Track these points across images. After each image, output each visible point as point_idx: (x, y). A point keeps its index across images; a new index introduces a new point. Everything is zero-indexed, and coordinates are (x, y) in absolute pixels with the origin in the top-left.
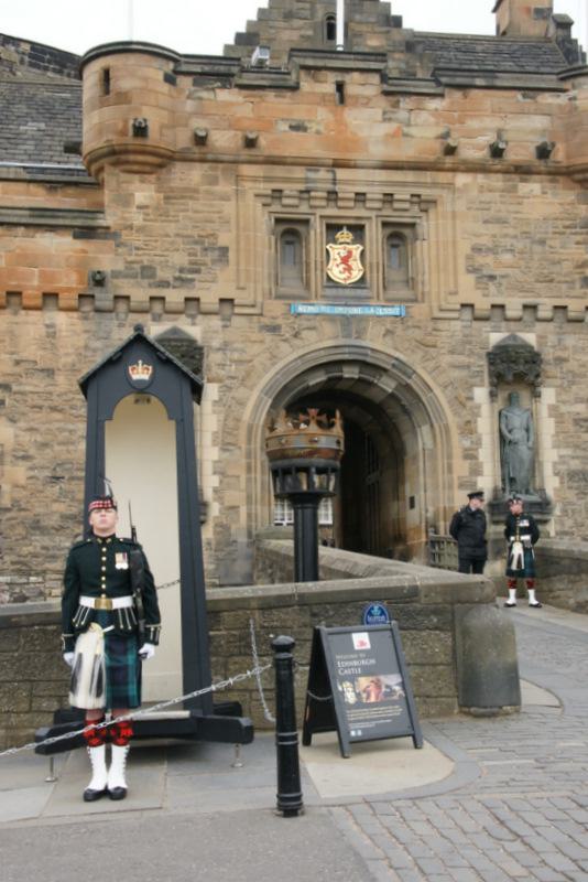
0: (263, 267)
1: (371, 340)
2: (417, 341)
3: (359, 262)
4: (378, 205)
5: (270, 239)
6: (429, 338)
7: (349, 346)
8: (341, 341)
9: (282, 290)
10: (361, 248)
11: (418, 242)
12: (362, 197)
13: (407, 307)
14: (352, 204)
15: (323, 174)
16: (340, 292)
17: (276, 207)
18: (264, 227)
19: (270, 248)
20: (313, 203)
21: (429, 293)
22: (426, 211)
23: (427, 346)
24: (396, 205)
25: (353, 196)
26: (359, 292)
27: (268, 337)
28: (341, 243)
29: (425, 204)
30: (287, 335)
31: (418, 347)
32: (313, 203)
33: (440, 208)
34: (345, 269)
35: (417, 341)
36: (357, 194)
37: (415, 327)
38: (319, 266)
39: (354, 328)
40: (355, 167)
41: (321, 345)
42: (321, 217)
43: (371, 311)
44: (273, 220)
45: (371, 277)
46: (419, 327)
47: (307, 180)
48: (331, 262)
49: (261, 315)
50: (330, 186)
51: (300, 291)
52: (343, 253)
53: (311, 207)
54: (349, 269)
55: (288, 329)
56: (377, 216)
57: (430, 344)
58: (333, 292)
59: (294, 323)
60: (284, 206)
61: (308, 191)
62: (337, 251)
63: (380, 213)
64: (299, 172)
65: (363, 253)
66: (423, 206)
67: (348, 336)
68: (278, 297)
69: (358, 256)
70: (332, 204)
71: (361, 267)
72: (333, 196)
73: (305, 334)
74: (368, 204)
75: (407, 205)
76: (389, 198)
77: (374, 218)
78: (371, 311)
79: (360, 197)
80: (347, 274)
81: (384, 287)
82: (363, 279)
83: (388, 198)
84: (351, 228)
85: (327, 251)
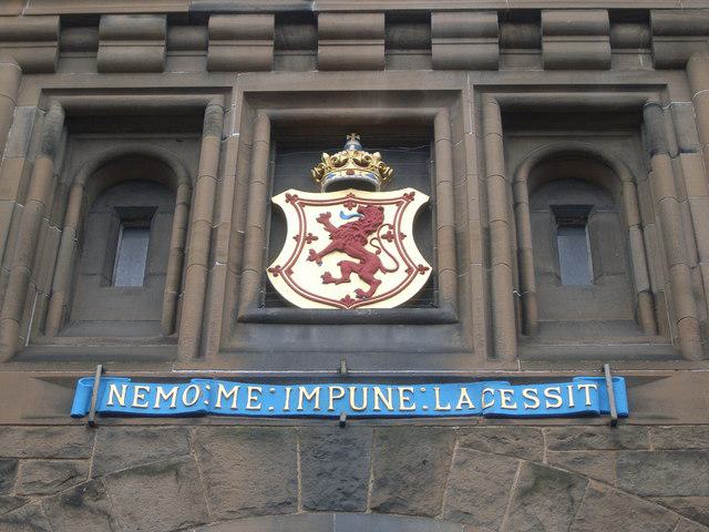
1: (461, 516)
3: (410, 243)
4: (489, 50)
5: (30, 170)
9: (63, 343)
10: (421, 199)
11: (661, 162)
13: (631, 383)
14: (376, 51)
20: (219, 52)
24: (553, 48)
26: (404, 336)
32: (219, 52)
34: (347, 269)
37: (675, 453)
38: (223, 245)
39: (371, 464)
42: (252, 98)
44: (56, 112)
45: (459, 284)
52: (340, 216)
53: (215, 68)
54: (368, 268)
55: (43, 475)
56: (479, 89)
58: (289, 336)
59: (74, 448)
60: (105, 69)
62: (312, 213)
65: (424, 218)
66: (664, 48)
69: (407, 226)
70: (299, 59)
71: (418, 258)
72: (302, 33)
73: (120, 494)
74: (441, 50)
75: (601, 48)
76: (526, 31)
77: (468, 95)
81: (524, 328)
84: (374, 136)
85: (277, 216)
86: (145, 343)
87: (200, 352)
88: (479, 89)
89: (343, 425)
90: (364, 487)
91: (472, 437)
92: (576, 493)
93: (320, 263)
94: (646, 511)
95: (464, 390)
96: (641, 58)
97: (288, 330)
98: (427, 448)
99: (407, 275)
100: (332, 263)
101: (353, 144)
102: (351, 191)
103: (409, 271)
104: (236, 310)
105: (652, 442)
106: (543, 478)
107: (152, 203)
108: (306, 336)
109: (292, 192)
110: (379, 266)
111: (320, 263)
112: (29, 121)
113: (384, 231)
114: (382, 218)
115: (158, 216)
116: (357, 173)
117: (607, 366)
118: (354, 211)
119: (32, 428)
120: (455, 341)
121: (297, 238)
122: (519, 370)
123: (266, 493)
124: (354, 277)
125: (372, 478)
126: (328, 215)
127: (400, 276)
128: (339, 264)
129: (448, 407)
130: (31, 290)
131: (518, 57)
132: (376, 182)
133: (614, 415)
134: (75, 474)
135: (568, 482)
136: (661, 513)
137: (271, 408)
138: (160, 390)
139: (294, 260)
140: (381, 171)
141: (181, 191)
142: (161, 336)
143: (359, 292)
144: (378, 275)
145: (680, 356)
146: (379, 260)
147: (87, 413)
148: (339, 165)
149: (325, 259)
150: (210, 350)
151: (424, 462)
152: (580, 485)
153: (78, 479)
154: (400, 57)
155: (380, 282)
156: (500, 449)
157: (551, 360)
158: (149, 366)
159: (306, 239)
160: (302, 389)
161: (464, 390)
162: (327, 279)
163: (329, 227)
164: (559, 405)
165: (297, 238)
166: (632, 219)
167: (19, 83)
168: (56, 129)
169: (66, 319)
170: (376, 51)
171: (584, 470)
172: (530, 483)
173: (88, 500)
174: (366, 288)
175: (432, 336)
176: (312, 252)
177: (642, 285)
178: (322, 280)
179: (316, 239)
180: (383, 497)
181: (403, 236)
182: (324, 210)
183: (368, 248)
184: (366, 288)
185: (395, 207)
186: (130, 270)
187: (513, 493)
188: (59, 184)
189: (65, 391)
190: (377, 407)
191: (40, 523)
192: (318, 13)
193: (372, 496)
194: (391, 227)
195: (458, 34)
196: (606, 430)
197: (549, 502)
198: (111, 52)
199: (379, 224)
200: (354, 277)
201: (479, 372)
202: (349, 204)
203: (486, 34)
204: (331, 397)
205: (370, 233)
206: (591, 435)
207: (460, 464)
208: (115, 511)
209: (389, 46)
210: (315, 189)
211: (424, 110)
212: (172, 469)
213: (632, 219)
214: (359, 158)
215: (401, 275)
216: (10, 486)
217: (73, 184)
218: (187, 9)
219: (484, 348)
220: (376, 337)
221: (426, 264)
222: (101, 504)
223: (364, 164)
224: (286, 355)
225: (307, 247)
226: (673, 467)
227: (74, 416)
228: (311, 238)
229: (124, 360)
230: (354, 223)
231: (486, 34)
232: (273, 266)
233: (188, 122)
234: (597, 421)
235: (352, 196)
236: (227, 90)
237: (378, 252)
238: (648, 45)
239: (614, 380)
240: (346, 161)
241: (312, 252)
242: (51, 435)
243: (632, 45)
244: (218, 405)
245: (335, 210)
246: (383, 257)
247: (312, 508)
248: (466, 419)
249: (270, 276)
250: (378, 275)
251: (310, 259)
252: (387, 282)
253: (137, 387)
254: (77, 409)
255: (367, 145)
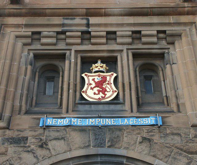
0: (16, 88)
1: (127, 148)
2: (176, 147)
3: (113, 85)
4: (129, 40)
5: (26, 69)
6: (190, 145)
7: (101, 155)
8: (92, 151)
9: (36, 109)
10: (115, 75)
11: (168, 66)
12: (113, 36)
13: (163, 118)
14: (104, 40)
15: (78, 20)
16: (93, 107)
17: (37, 46)
18: (23, 60)
19: (25, 75)
21: (184, 104)
22: (173, 43)
23: (192, 153)
24: (144, 39)
25: (104, 34)
26: (112, 107)
27: (11, 149)
28: (96, 72)
29: (173, 39)
30: (33, 147)
31: (180, 154)
33: (184, 39)
34: (99, 91)
35: (176, 147)
36: (108, 33)
37: (173, 134)
38: (72, 86)
40: (106, 15)
41: (69, 155)
42: (76, 51)
43: (126, 122)
44: (31, 55)
46: (179, 134)
47: (63, 25)
48: (86, 86)
49: (8, 128)
50: (84, 29)
51: (56, 110)
52: (97, 79)
53: (67, 44)
54: (104, 91)
55: (33, 140)
56: (128, 49)
57: (191, 150)
58: (87, 107)
59: (40, 134)
60: (43, 45)
61: (63, 33)
62: (91, 78)
63: (130, 47)
64: (57, 20)
66: (169, 39)
67: (101, 145)
68: (27, 112)
69: (112, 81)
71: (115, 89)
72: (87, 36)
73: (51, 145)
74: (119, 40)
75: (155, 39)
76: (138, 35)
77: (125, 51)
78: (126, 122)
79: (111, 36)
80: (101, 94)
81: (139, 105)
82: (117, 97)
83: (137, 35)
84: (104, 60)
85: (83, 79)
86: (55, 109)
87: (67, 112)
88: (128, 49)
89: (100, 128)
90: (105, 142)
91: (128, 130)
92: (151, 143)
93: (93, 90)
94: (167, 147)
95: (126, 120)
96: (164, 41)
97: (87, 106)
98: (118, 133)
99: (112, 93)
100: (96, 90)
101: (99, 62)
102: (99, 73)
103: (113, 92)
104: (75, 101)
105: (168, 131)
106: (144, 139)
107: (54, 75)
108: (91, 107)
109: (86, 73)
110: (106, 90)
111: (93, 90)
112: (26, 57)
113: (107, 82)
114: (106, 79)
115: (56, 79)
116: (100, 69)
117: (157, 114)
118: (100, 78)
119: (31, 129)
120: (124, 109)
121: (88, 84)
122: (138, 115)
123: (84, 144)
124: (101, 93)
125: (107, 140)
126: (94, 79)
127: (111, 94)
128: (97, 90)
129: (123, 123)
130: (28, 97)
131: (136, 41)
132: (105, 71)
133: (159, 125)
134: (41, 140)
135: (149, 140)
136: (171, 147)
137: (83, 124)
138: (59, 120)
139: (87, 89)
140: (106, 68)
141: (61, 73)
142: (58, 107)
143: (102, 96)
144: (106, 93)
145: (172, 112)
146: (106, 89)
147: (43, 126)
148: (96, 67)
149: (94, 89)
150: (70, 111)
151: (118, 136)
152: (152, 141)
153: (42, 141)
154: (110, 42)
155: (106, 94)
156: (135, 133)
157: (145, 112)
158: (56, 114)
159: (90, 84)
160: (91, 120)
161: (126, 120)
162: (95, 94)
163: (95, 82)
164: (147, 123)
165: (88, 84)
166: (162, 79)
167: (23, 47)
168: (32, 59)
169: (36, 103)
170: (104, 40)
171: (153, 138)
172: (141, 141)
173: (44, 146)
174: (103, 96)
175: (118, 107)
176: (91, 87)
177: (164, 94)
178: (93, 94)
179: (92, 84)
180: (109, 144)
181: (111, 84)
182: (93, 78)
183: (104, 86)
184: (103, 96)
185: (109, 77)
186: (49, 91)
187: (138, 143)
188: (33, 72)
189: (38, 121)
190: (107, 124)
191: (34, 152)
192: (91, 31)
193: (108, 144)
194: (109, 81)
195: (122, 36)
196: (157, 128)
197: (145, 145)
198: (44, 40)
199: (105, 81)
200: (101, 93)
201: (129, 115)
202: (99, 76)
203: (129, 36)
204: (97, 122)
205: (104, 83)
206: (154, 130)
207: (126, 136)
208: (51, 148)
209: (107, 39)
210: (91, 73)
211: (115, 54)
212: (63, 138)
213: (162, 79)
214: (101, 65)
215: (111, 93)
216: (27, 143)
217: (36, 71)
218: (61, 31)
219: (130, 110)
220: (106, 107)
221: (116, 90)
222: (48, 147)
223: (102, 67)
224: (87, 112)
225: (90, 86)
226: (172, 137)
227: (40, 127)
228: (91, 84)
229: (51, 113)
230: (100, 81)
231: (129, 36)
232: (83, 91)
233: (62, 57)
234: (155, 126)
235: (99, 74)
236: (70, 50)
237: (106, 87)
238: (166, 38)
239: (159, 117)
240: (98, 66)
241: (91, 87)
242: (35, 131)
243: (162, 38)
244: (72, 124)
245: (96, 78)
246: (107, 88)
247: (94, 147)
248: (127, 126)
249: (82, 93)
250: (106, 93)
251: (91, 89)
252: (108, 94)
253: (54, 120)
254: (41, 125)
255: (102, 62)
